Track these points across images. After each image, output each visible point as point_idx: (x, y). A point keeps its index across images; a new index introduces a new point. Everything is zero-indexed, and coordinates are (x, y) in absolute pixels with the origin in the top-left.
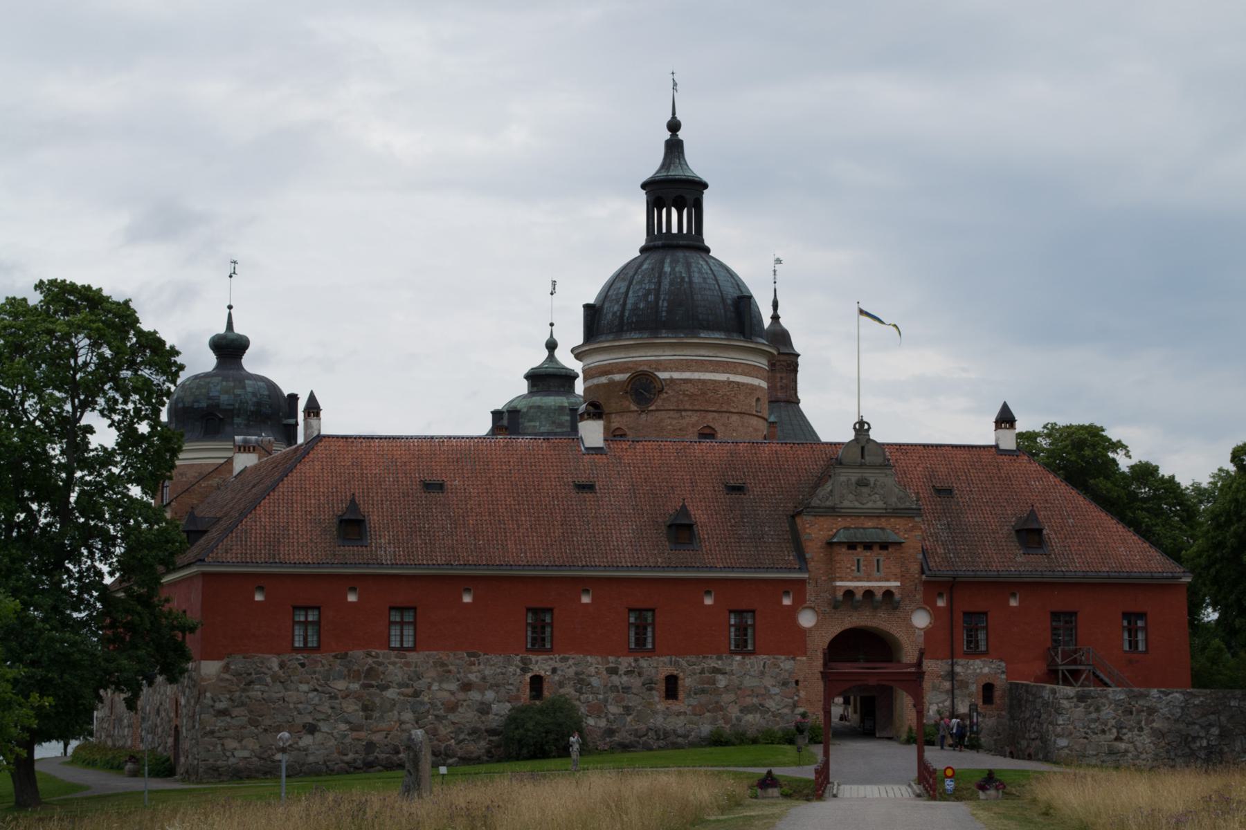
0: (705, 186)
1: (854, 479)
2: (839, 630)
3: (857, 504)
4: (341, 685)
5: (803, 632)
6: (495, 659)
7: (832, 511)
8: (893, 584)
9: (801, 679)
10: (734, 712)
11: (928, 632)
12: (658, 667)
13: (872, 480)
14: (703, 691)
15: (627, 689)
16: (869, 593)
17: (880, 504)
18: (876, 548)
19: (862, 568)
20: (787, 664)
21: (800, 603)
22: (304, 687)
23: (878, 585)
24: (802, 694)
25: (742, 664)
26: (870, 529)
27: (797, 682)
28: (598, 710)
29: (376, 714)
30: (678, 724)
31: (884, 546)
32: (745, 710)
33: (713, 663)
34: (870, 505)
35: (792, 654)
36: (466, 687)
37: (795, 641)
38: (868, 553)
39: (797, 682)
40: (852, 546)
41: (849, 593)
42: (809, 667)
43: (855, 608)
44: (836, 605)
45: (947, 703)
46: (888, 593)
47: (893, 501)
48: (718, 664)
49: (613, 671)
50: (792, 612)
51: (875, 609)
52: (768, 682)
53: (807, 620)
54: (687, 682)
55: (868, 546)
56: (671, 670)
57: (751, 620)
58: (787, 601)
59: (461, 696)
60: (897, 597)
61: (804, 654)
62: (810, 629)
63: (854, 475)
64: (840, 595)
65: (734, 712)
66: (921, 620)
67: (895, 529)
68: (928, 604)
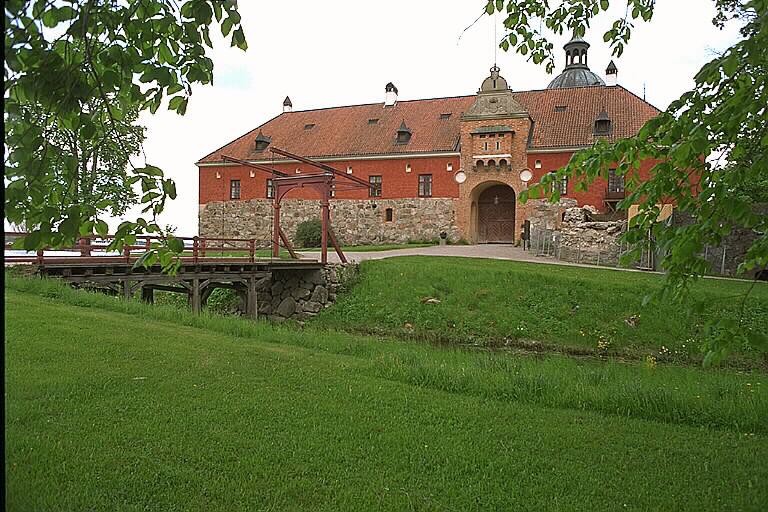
0: (589, 46)
4: (247, 214)
6: (309, 202)
7: (476, 119)
10: (419, 228)
12: (382, 204)
14: (405, 217)
15: (367, 216)
16: (491, 162)
20: (447, 201)
21: (456, 170)
22: (234, 216)
24: (456, 218)
25: (424, 202)
26: (497, 125)
28: (353, 227)
29: (261, 227)
30: (391, 234)
31: (501, 134)
32: (426, 226)
33: (409, 201)
36: (297, 215)
37: (453, 190)
40: (482, 135)
41: (480, 162)
42: (464, 203)
44: (475, 169)
46: (503, 161)
48: (413, 203)
49: (362, 207)
52: (438, 211)
53: (460, 178)
54: (396, 212)
55: (492, 135)
56: (388, 206)
57: (431, 177)
58: (450, 169)
59: (294, 219)
60: (508, 163)
63: (490, 97)
65: (419, 228)
66: (526, 176)
67: (506, 125)
68: (531, 166)
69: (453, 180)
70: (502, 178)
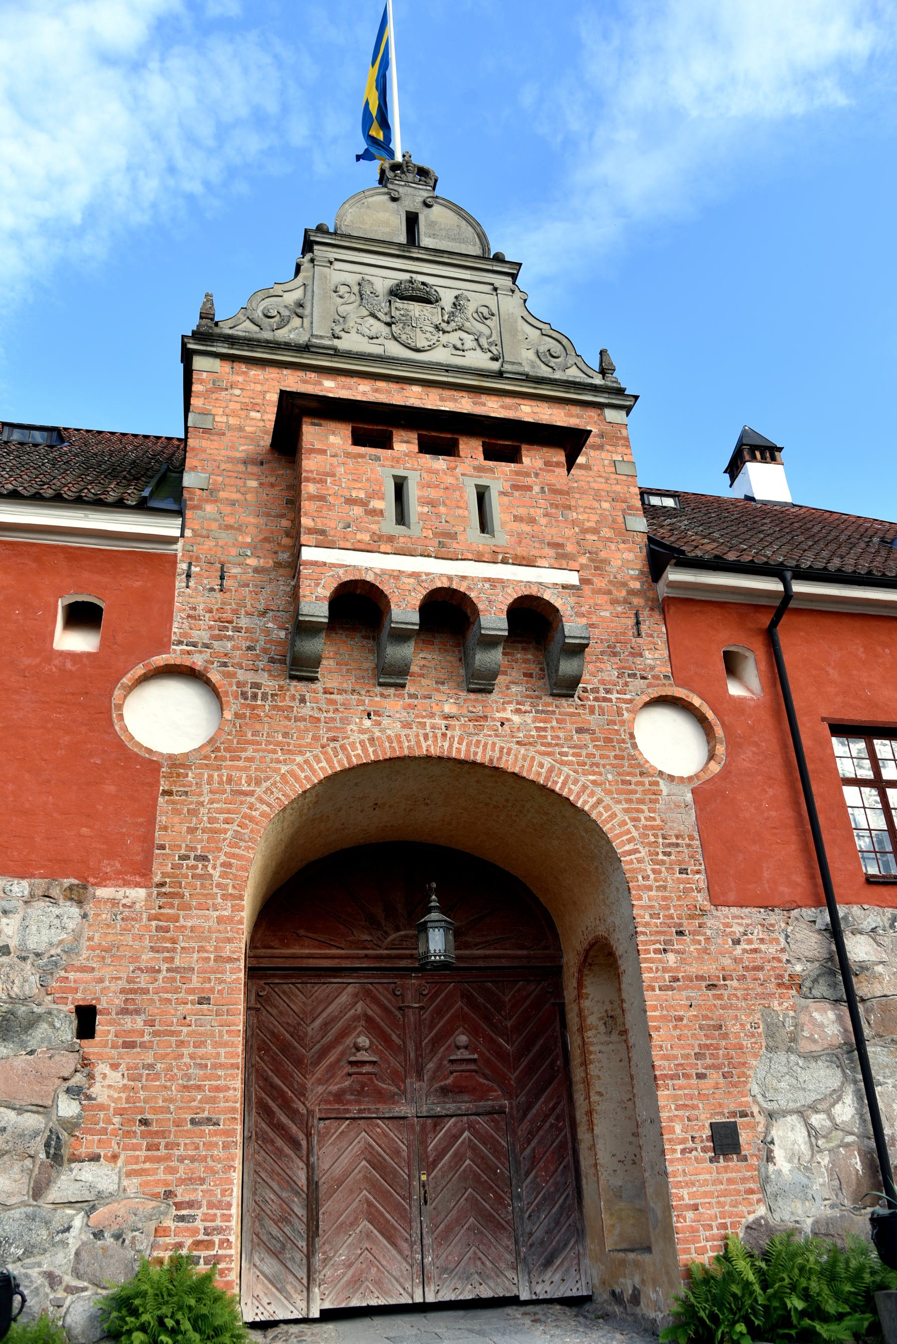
1: (382, 283)
2: (322, 769)
3: (395, 350)
5: (145, 774)
8: (547, 579)
9: (108, 1001)
11: (707, 794)
13: (447, 298)
16: (447, 613)
17: (479, 360)
18: (471, 449)
19: (415, 508)
23: (492, 582)
24: (108, 1084)
27: (86, 1020)
34: (440, 355)
35: (71, 872)
38: (440, 463)
39: (86, 1020)
41: (358, 607)
43: (393, 676)
45: (847, 1110)
46: (532, 620)
47: (525, 358)
50: (93, 694)
51: (481, 683)
53: (163, 719)
55: (440, 433)
61: (140, 871)
62: (178, 763)
64: (315, 605)
69: (103, 716)
70: (505, 730)
